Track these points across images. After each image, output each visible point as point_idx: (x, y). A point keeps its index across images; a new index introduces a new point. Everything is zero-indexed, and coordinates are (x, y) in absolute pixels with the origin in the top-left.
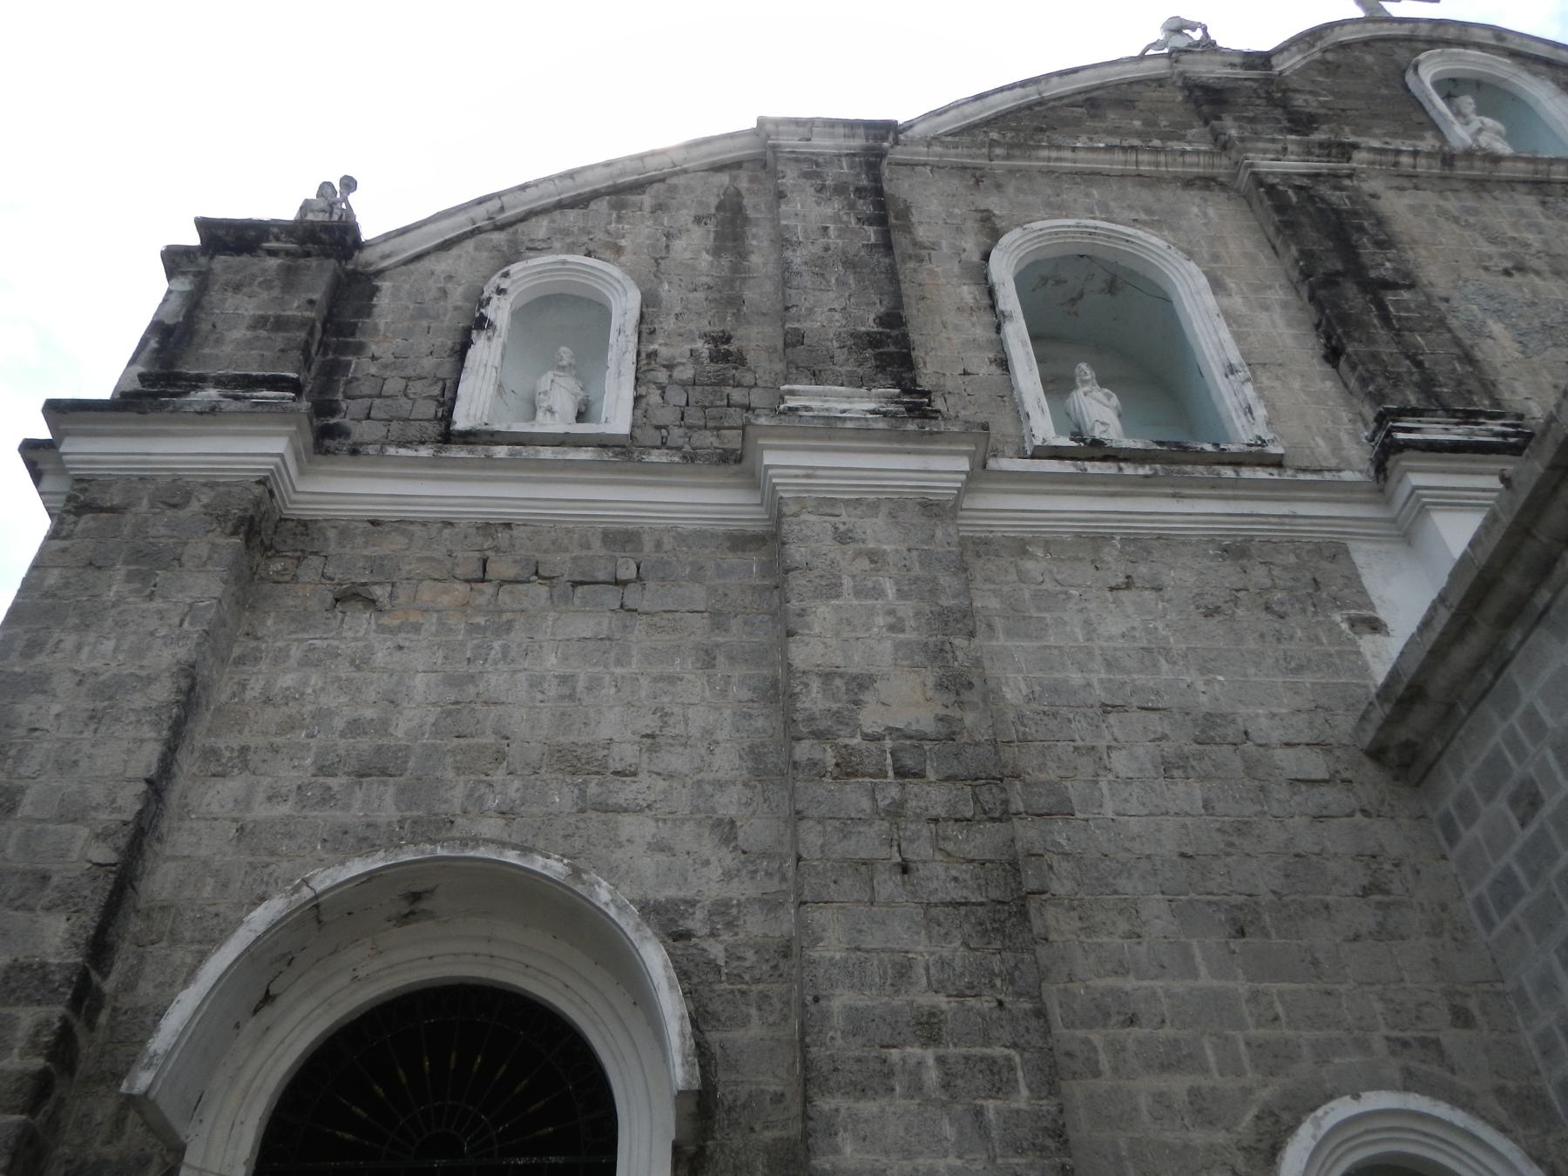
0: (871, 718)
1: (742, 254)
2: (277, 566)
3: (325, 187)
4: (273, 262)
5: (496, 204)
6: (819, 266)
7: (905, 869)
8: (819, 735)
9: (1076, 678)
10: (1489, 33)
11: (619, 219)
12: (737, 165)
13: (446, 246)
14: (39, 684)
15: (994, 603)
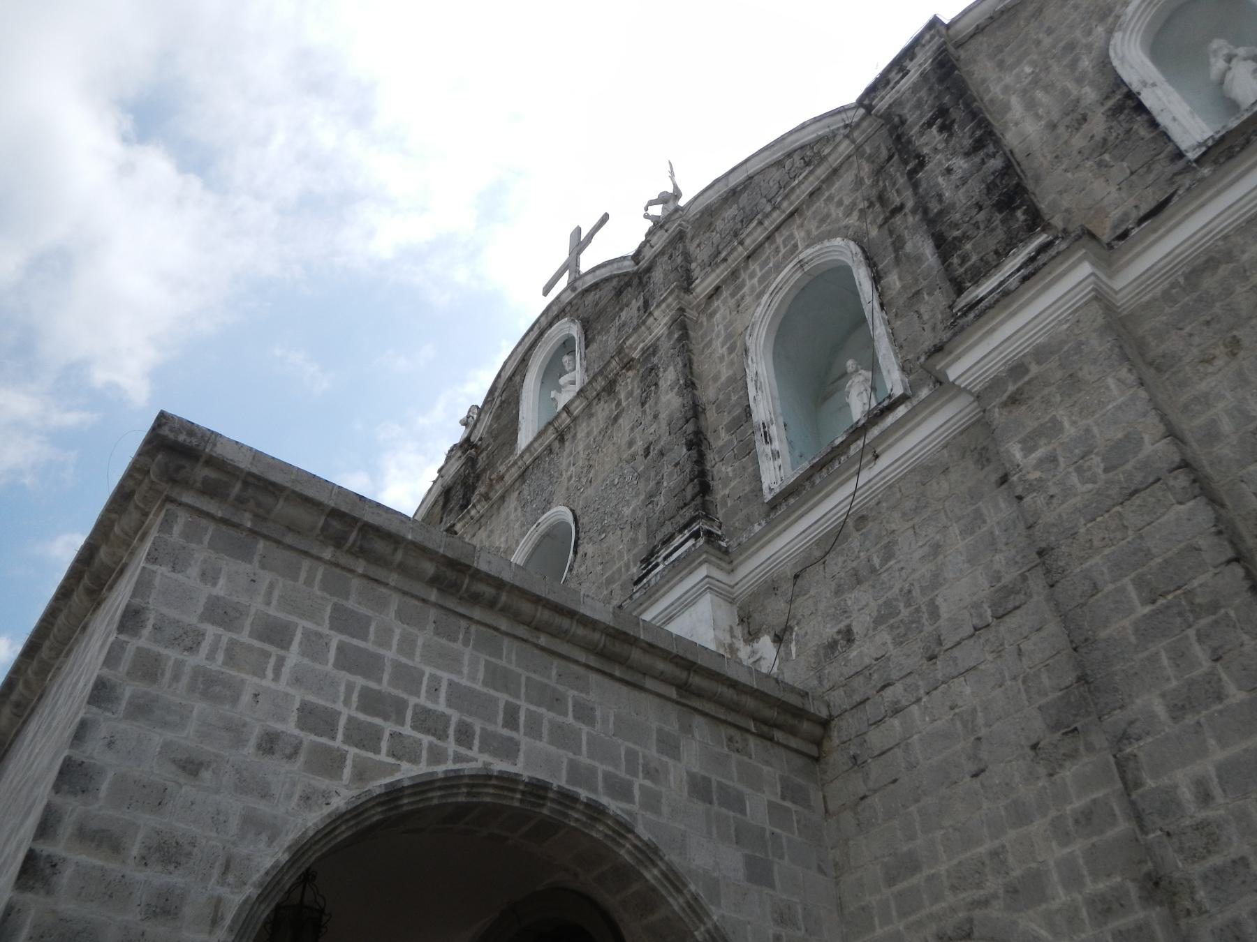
10: (569, 291)
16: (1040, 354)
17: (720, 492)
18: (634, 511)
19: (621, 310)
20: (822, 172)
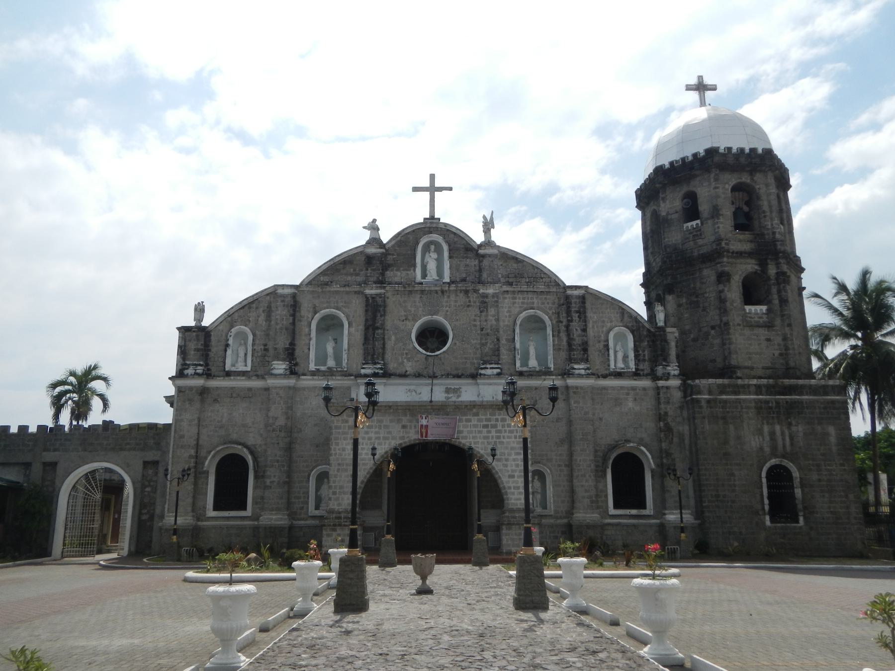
0: (277, 424)
1: (270, 321)
2: (205, 395)
3: (199, 303)
4: (194, 334)
5: (227, 313)
6: (281, 329)
8: (271, 426)
9: (307, 412)
11: (250, 312)
12: (271, 293)
13: (221, 322)
14: (182, 420)
15: (299, 400)
16: (582, 388)
17: (501, 357)
18: (476, 343)
19: (467, 257)
20: (547, 290)
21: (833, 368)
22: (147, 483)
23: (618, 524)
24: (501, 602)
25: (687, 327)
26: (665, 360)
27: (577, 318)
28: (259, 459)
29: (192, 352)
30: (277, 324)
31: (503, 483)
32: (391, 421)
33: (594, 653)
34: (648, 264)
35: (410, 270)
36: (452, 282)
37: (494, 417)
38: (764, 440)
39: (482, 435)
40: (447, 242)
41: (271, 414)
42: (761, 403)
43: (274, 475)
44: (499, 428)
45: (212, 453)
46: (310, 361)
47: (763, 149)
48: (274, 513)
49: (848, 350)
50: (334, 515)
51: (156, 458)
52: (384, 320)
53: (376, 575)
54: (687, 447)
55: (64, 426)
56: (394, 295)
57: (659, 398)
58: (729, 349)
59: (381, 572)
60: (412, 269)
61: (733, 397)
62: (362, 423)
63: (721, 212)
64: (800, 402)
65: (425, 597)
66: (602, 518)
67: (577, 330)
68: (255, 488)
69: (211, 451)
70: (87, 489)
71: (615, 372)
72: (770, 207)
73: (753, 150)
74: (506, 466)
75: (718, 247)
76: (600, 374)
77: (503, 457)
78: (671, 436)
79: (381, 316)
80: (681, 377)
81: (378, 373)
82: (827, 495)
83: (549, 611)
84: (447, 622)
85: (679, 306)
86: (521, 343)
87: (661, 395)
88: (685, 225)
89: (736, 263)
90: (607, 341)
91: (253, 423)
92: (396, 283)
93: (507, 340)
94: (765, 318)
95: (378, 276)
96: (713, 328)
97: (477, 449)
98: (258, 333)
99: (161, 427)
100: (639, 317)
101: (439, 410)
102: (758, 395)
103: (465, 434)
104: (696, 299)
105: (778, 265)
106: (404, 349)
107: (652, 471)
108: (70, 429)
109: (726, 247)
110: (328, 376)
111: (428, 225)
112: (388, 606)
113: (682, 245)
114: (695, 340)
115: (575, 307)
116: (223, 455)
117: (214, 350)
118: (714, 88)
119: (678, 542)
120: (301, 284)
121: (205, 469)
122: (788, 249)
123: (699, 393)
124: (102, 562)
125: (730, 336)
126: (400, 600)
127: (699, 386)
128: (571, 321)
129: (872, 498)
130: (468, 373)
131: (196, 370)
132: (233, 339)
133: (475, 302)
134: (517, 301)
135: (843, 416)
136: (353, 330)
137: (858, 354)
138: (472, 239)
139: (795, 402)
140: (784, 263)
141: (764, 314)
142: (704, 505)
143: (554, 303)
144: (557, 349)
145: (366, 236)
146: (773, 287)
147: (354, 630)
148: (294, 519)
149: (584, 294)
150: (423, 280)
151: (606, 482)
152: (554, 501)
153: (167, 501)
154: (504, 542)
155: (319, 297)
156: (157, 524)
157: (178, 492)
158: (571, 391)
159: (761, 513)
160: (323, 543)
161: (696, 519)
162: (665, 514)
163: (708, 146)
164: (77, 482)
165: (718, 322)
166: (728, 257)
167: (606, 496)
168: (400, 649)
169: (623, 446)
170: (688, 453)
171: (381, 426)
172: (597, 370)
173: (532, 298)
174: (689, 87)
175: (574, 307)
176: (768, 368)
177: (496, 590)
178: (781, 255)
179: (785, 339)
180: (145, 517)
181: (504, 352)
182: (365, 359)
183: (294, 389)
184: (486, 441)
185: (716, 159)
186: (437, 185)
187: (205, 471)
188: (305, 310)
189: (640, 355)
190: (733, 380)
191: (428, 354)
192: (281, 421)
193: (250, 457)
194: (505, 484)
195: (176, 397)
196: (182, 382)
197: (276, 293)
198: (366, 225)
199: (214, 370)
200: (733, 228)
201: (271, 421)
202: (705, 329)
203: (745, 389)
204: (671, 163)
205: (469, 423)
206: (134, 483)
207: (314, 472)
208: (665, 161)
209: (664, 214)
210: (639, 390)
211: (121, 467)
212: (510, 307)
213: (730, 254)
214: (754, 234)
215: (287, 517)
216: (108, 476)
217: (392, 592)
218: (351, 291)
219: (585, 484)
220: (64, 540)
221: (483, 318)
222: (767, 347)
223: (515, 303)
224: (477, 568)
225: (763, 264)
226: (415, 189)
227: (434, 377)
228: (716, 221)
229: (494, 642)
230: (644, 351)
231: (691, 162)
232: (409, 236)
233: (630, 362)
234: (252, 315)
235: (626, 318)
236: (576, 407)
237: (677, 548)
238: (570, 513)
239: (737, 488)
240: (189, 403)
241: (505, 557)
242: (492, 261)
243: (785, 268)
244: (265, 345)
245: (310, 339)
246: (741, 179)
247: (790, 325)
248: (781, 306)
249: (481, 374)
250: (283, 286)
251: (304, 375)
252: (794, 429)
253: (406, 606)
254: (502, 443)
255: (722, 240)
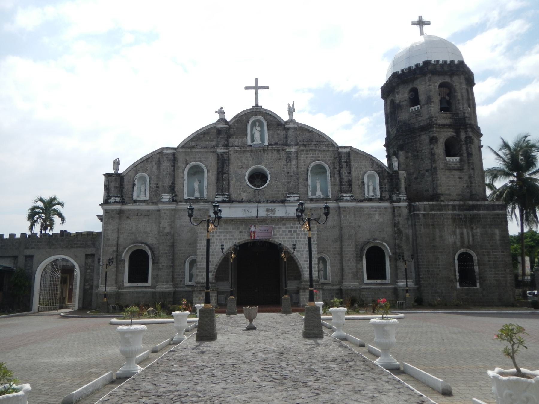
0: (165, 231)
1: (160, 170)
2: (122, 215)
3: (116, 159)
4: (114, 178)
5: (134, 165)
6: (166, 174)
7: (166, 243)
8: (162, 232)
9: (183, 224)
12: (160, 153)
14: (108, 230)
16: (348, 208)
17: (300, 190)
18: (284, 182)
19: (279, 130)
21: (499, 194)
22: (88, 267)
23: (370, 288)
24: (296, 334)
25: (412, 171)
26: (398, 190)
27: (345, 166)
28: (154, 252)
29: (113, 189)
30: (164, 171)
31: (301, 265)
32: (233, 229)
33: (347, 362)
34: (388, 133)
35: (244, 138)
36: (270, 145)
37: (295, 226)
38: (456, 238)
39: (288, 237)
40: (266, 120)
41: (161, 225)
42: (455, 215)
43: (164, 261)
44: (298, 232)
45: (127, 249)
46: (184, 194)
47: (458, 61)
48: (164, 284)
49: (508, 183)
50: (200, 285)
51: (93, 252)
52: (228, 168)
53: (224, 320)
54: (411, 242)
55: (37, 234)
56: (234, 153)
57: (394, 214)
58: (437, 183)
59: (227, 317)
60: (245, 137)
61: (439, 212)
62: (212, 229)
63: (432, 101)
64: (479, 215)
65: (251, 332)
66: (360, 285)
67: (345, 173)
68: (153, 269)
69: (126, 248)
70: (52, 271)
71: (368, 198)
72: (462, 96)
73: (452, 62)
74: (302, 255)
75: (430, 122)
76: (359, 199)
77: (301, 250)
78: (401, 236)
79: (227, 166)
80: (407, 201)
81: (225, 200)
82: (493, 270)
83: (323, 339)
84: (262, 346)
85: (407, 158)
86: (311, 181)
87: (396, 212)
88: (411, 109)
89: (441, 132)
90: (363, 179)
91: (151, 231)
92: (236, 146)
93: (304, 180)
94: (458, 165)
95: (224, 141)
96: (427, 171)
97: (285, 245)
98: (152, 177)
99: (96, 234)
100: (382, 165)
101: (262, 222)
102: (453, 211)
103: (278, 236)
104: (417, 154)
105: (466, 132)
106: (241, 186)
107: (390, 257)
108: (41, 236)
109: (435, 122)
110: (195, 202)
111: (255, 110)
112: (229, 337)
113: (409, 120)
114: (416, 178)
115: (344, 159)
116: (133, 250)
117: (126, 187)
118: (428, 23)
119: (405, 299)
120: (178, 147)
121: (122, 258)
122: (473, 122)
123: (419, 210)
124: (62, 314)
125: (437, 176)
126: (236, 333)
127: (418, 206)
128: (342, 167)
129: (520, 271)
130: (280, 200)
131: (115, 199)
132: (138, 180)
133: (283, 157)
134: (309, 156)
135: (504, 223)
136: (210, 174)
137: (514, 185)
138: (281, 119)
139: (476, 215)
140: (470, 131)
141: (457, 162)
142: (420, 276)
143: (331, 157)
144: (333, 184)
145: (217, 117)
146: (463, 146)
147: (207, 350)
148: (176, 287)
149: (349, 151)
150: (252, 144)
151: (362, 264)
152: (332, 275)
153: (100, 277)
154: (301, 299)
155: (189, 154)
156: (95, 291)
157: (106, 272)
158: (342, 210)
159: (454, 281)
160: (194, 301)
161: (415, 285)
162: (397, 282)
163: (425, 59)
164: (46, 267)
165: (430, 167)
166: (436, 128)
167: (362, 272)
168: (232, 361)
169: (372, 242)
170: (411, 246)
171: (227, 232)
172: (357, 197)
173: (318, 154)
174: (413, 23)
175: (344, 159)
176: (459, 195)
177: (294, 327)
178: (468, 126)
179: (470, 177)
180: (87, 287)
181: (301, 186)
182: (217, 192)
183: (175, 210)
184: (290, 240)
185: (430, 67)
186: (259, 86)
187: (123, 260)
188: (180, 164)
189: (383, 188)
190: (439, 202)
191: (256, 188)
192: (168, 230)
193: (149, 251)
194: (302, 266)
195: (104, 215)
196: (107, 207)
197: (163, 153)
198: (217, 111)
199: (126, 199)
200: (440, 110)
201: (161, 230)
202: (422, 172)
203: (446, 207)
204: (402, 71)
205: (280, 230)
206: (80, 267)
207: (188, 259)
208: (399, 70)
209: (398, 102)
210: (383, 208)
211: (72, 258)
212: (304, 160)
213: (438, 126)
214: (452, 114)
215: (172, 286)
216: (64, 263)
217: (232, 329)
218: (208, 151)
219: (350, 265)
220: (39, 301)
221: (288, 166)
222: (459, 182)
223: (308, 157)
224: (285, 315)
225: (458, 132)
226: (247, 88)
227: (259, 202)
228: (429, 106)
229: (288, 357)
230: (385, 185)
231: (415, 70)
232: (243, 117)
233: (377, 192)
234: (149, 166)
235: (375, 166)
236: (345, 219)
237: (404, 302)
238: (341, 283)
239: (440, 266)
240: (112, 220)
241: (302, 308)
242: (294, 132)
243: (471, 134)
244: (157, 184)
245: (184, 180)
246: (445, 80)
247: (473, 169)
248: (468, 157)
249: (287, 200)
250: (167, 148)
251: (181, 202)
252: (475, 231)
253: (240, 336)
254: (299, 241)
255: (433, 117)
